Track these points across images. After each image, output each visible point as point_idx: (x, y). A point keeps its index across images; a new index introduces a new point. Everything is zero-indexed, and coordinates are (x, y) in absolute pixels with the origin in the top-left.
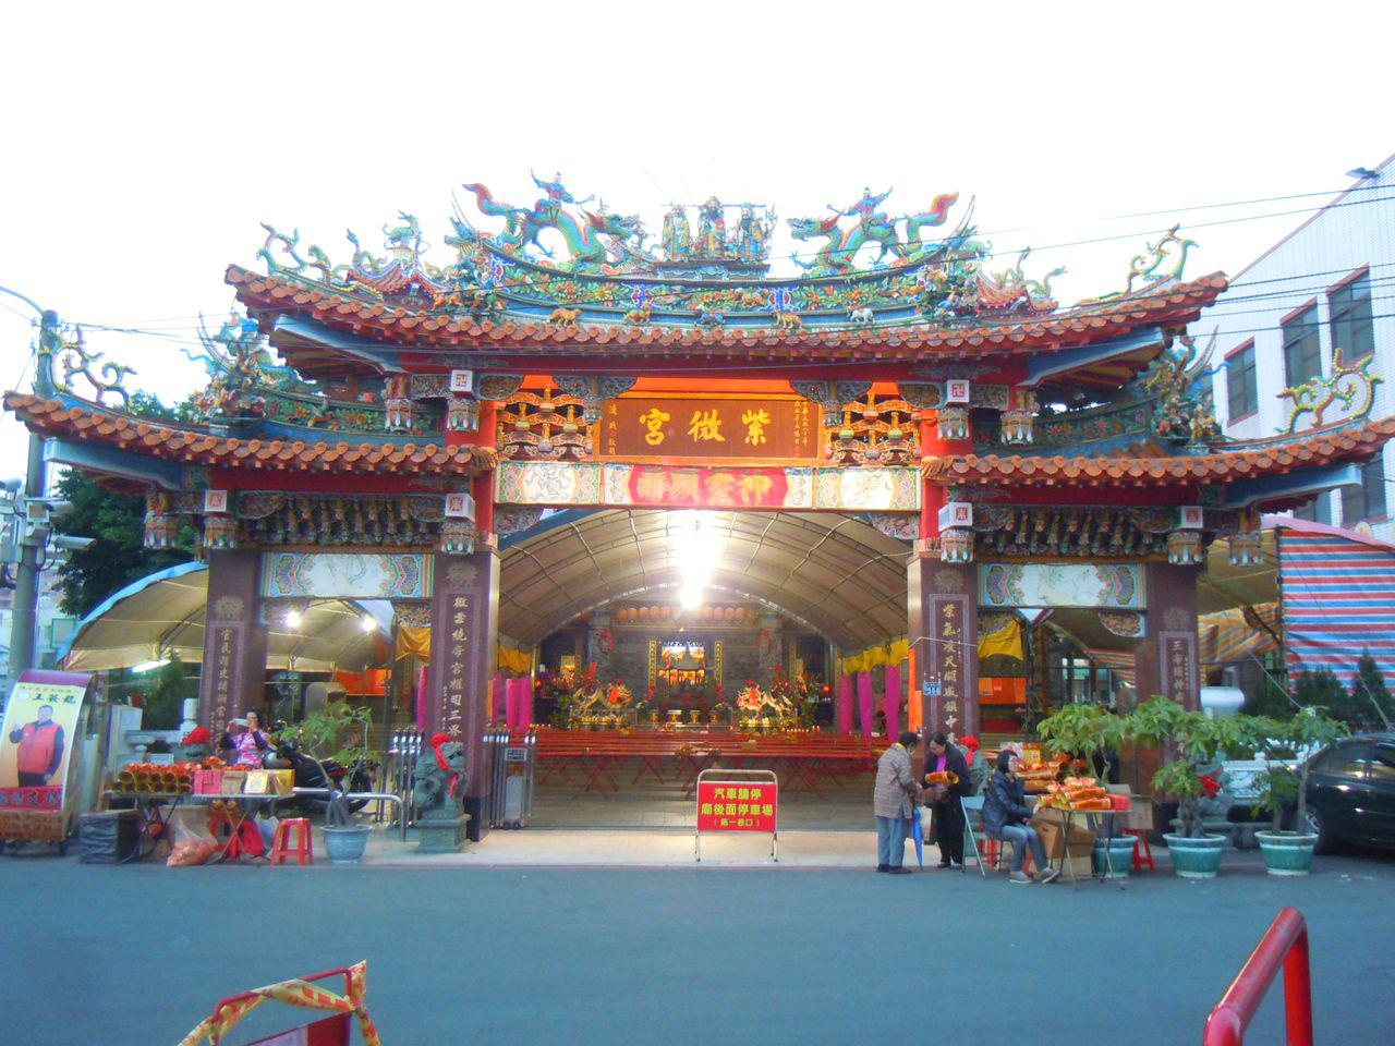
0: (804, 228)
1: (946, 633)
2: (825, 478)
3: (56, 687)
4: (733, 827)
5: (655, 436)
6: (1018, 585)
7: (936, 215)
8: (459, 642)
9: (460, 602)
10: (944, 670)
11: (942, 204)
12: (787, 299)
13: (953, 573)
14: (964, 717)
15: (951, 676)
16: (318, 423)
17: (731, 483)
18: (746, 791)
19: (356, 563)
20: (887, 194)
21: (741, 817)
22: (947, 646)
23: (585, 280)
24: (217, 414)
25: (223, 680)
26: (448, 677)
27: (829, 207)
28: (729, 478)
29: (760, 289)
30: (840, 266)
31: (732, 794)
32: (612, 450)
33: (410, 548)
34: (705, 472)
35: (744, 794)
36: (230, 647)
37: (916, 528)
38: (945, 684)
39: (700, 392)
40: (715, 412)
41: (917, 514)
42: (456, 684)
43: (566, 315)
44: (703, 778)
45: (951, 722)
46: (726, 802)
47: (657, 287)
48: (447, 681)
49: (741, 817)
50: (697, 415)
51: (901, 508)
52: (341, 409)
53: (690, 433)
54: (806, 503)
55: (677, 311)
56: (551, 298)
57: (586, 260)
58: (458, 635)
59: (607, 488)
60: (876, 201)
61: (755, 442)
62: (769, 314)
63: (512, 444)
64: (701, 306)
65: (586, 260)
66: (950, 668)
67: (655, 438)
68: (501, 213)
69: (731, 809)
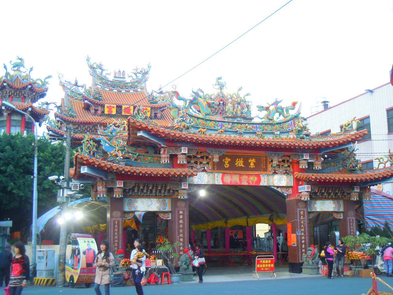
0: (261, 108)
1: (301, 219)
2: (270, 177)
3: (89, 239)
4: (264, 270)
5: (227, 165)
6: (315, 206)
7: (293, 107)
8: (182, 224)
9: (181, 212)
10: (301, 228)
11: (294, 104)
12: (258, 128)
13: (303, 203)
14: (306, 240)
15: (303, 230)
16: (135, 160)
17: (247, 179)
18: (267, 261)
19: (149, 201)
20: (281, 101)
21: (266, 267)
22: (302, 222)
23: (207, 120)
24: (121, 159)
25: (116, 235)
26: (179, 233)
27: (268, 103)
28: (247, 177)
29: (251, 125)
30: (271, 120)
31: (264, 262)
32: (216, 169)
33: (165, 197)
34: (240, 175)
35: (267, 262)
36: (117, 226)
37: (291, 191)
38: (302, 232)
39: (238, 153)
40: (242, 159)
41: (291, 187)
42: (181, 235)
43: (203, 130)
44: (258, 258)
45: (303, 242)
46: (262, 264)
47: (225, 123)
48: (179, 235)
49: (266, 267)
50: (238, 159)
51: (288, 185)
52: (141, 155)
53: (236, 164)
54: (265, 184)
55: (231, 130)
56: (197, 125)
57: (207, 114)
58: (181, 221)
59: (216, 179)
60: (279, 102)
61: (252, 167)
62: (254, 132)
63: (202, 167)
64: (238, 129)
65: (207, 114)
66: (303, 228)
67: (227, 166)
68: (183, 100)
69: (264, 266)
